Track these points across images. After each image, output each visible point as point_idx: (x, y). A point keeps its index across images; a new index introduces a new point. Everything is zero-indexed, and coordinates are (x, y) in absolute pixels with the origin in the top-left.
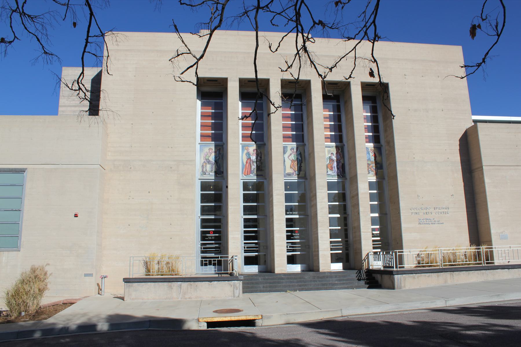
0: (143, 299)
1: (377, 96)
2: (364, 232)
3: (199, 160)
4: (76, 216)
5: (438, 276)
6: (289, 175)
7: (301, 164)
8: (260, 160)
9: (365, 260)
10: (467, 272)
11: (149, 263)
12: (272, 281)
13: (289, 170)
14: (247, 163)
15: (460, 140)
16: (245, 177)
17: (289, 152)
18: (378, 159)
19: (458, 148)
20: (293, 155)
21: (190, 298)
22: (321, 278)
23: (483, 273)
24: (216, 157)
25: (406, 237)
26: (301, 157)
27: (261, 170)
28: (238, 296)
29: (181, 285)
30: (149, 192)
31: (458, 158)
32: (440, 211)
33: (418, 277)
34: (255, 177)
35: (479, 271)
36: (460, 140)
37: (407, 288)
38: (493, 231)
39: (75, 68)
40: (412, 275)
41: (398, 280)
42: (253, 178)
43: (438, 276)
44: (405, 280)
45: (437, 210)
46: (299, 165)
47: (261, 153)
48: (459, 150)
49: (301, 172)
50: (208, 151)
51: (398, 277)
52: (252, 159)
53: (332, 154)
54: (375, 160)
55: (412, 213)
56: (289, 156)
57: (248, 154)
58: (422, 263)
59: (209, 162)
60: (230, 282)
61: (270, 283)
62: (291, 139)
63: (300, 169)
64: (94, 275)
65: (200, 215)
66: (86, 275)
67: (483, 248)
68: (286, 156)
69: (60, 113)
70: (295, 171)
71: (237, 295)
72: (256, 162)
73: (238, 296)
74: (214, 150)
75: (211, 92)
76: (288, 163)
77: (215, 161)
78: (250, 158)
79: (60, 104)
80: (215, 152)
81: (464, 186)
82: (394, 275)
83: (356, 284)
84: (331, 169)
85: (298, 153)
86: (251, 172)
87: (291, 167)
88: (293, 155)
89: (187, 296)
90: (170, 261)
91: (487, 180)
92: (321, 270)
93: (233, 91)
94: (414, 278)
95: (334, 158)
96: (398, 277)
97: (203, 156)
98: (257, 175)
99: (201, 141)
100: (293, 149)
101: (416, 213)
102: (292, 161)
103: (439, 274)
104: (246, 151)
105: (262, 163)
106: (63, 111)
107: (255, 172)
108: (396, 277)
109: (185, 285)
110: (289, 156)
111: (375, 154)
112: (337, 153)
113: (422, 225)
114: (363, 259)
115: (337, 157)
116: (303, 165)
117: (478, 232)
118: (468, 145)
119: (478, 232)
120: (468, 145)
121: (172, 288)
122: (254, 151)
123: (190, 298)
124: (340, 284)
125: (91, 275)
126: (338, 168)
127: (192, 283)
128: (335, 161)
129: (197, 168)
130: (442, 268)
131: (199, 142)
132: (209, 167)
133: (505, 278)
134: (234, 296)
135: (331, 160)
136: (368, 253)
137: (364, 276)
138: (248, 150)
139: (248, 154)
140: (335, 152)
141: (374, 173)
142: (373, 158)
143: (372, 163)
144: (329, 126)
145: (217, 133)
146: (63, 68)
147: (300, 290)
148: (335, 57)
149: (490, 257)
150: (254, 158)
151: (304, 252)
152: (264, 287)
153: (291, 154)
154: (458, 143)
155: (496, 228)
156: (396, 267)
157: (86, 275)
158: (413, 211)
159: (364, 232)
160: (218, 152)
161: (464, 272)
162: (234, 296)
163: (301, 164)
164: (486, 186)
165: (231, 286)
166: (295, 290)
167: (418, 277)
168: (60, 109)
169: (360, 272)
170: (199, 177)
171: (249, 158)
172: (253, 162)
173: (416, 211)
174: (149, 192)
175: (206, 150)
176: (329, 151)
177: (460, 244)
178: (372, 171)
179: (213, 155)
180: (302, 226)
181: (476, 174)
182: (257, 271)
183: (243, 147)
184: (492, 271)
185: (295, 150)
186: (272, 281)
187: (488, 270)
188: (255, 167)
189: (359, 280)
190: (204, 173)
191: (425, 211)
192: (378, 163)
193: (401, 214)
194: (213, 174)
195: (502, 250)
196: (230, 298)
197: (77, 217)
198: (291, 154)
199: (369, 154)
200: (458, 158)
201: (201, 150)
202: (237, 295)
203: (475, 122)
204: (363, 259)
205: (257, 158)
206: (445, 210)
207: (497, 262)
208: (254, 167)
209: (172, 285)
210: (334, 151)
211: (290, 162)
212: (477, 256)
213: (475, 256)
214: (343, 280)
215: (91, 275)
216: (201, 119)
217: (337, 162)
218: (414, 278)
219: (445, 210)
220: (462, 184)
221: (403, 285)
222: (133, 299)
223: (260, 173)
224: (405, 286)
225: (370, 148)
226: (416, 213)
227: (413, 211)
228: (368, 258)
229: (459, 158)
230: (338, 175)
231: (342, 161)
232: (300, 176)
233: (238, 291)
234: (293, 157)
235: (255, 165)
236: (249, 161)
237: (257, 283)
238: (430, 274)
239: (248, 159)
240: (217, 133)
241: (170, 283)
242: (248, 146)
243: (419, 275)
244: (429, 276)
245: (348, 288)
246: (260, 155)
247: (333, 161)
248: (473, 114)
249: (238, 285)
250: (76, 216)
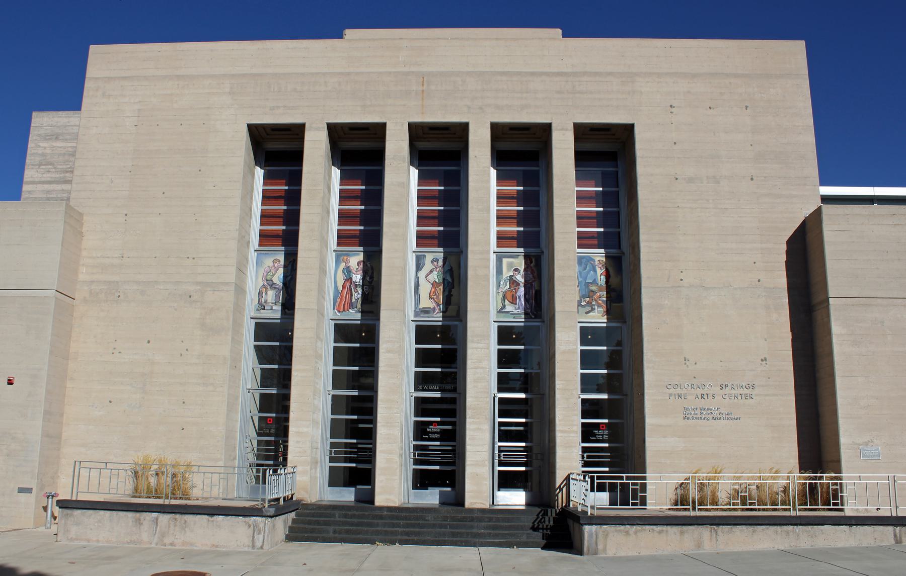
0: (88, 541)
1: (608, 151)
2: (562, 432)
3: (253, 281)
4: (10, 382)
5: (682, 533)
6: (426, 311)
7: (450, 291)
8: (370, 282)
9: (561, 490)
10: (751, 528)
11: (179, 478)
12: (356, 520)
13: (426, 303)
14: (343, 287)
15: (788, 242)
16: (339, 315)
17: (428, 266)
18: (614, 280)
19: (784, 258)
20: (435, 273)
21: (171, 544)
22: (459, 520)
23: (788, 533)
24: (285, 277)
25: (654, 444)
26: (452, 276)
27: (372, 302)
28: (262, 547)
29: (157, 519)
30: (149, 342)
31: (783, 281)
32: (733, 392)
33: (636, 533)
34: (359, 316)
35: (778, 528)
36: (790, 242)
37: (611, 553)
38: (843, 440)
39: (54, 113)
40: (622, 527)
41: (591, 535)
42: (354, 316)
43: (682, 533)
44: (606, 536)
45: (728, 391)
46: (446, 293)
47: (372, 268)
48: (787, 263)
49: (450, 307)
50: (271, 264)
51: (591, 531)
52: (354, 280)
53: (516, 270)
54: (607, 282)
55: (670, 395)
56: (428, 275)
57: (348, 270)
58: (751, 504)
59: (272, 285)
60: (247, 519)
61: (352, 524)
62: (515, 242)
63: (448, 301)
64: (34, 491)
65: (330, 389)
66: (21, 490)
67: (826, 478)
68: (422, 274)
69: (24, 195)
70: (438, 305)
71: (258, 544)
72: (363, 285)
73: (262, 547)
74: (282, 263)
75: (277, 149)
76: (425, 288)
77: (284, 284)
78: (351, 279)
79: (25, 180)
80: (285, 267)
81: (793, 341)
82: (583, 525)
83: (524, 539)
84: (513, 301)
85: (447, 268)
86: (351, 306)
87: (430, 297)
88: (435, 273)
89: (167, 541)
90: (175, 470)
91: (836, 329)
92: (468, 504)
93: (397, 146)
94: (627, 533)
95: (520, 278)
96: (591, 531)
97: (261, 273)
98: (362, 312)
99: (260, 245)
100: (437, 261)
101: (680, 396)
102: (434, 284)
103: (685, 528)
104: (343, 265)
105: (373, 288)
106: (29, 192)
107: (359, 306)
108: (587, 529)
109: (164, 518)
110: (428, 275)
111: (607, 270)
112: (525, 270)
113: (690, 422)
114: (557, 486)
115: (526, 277)
116: (454, 292)
117: (817, 443)
118: (804, 253)
119: (817, 443)
120: (804, 253)
121: (141, 524)
122: (358, 264)
123: (171, 544)
124: (490, 535)
125: (29, 490)
126: (526, 300)
127: (178, 516)
128: (522, 285)
129: (248, 298)
130: (796, 517)
131: (257, 247)
132: (271, 295)
133: (840, 545)
134: (253, 547)
135: (513, 282)
136: (569, 475)
137: (549, 522)
138: (346, 262)
139: (348, 270)
140: (522, 268)
141: (602, 310)
142: (602, 280)
143: (600, 290)
144: (515, 215)
145: (283, 228)
146: (34, 114)
147: (402, 542)
148: (490, 73)
149: (834, 497)
150: (357, 278)
151: (440, 466)
152: (335, 532)
153: (431, 271)
154: (784, 247)
155: (849, 436)
156: (694, 509)
157: (21, 490)
158: (672, 391)
159: (562, 432)
160: (290, 267)
161: (744, 527)
162: (253, 547)
163: (450, 291)
164: (835, 340)
165: (250, 526)
166: (393, 543)
167: (636, 533)
168: (25, 188)
169: (546, 514)
170: (253, 314)
171: (349, 279)
172: (356, 286)
173: (679, 391)
174: (149, 342)
175: (268, 262)
176: (510, 265)
177: (778, 463)
178: (600, 306)
179: (281, 271)
180: (440, 413)
181: (818, 315)
182: (352, 498)
183: (338, 257)
184: (810, 527)
185: (441, 263)
186: (356, 520)
187: (801, 524)
188: (360, 296)
189: (534, 529)
190: (262, 306)
191: (699, 392)
192: (614, 290)
193: (646, 397)
194: (280, 308)
195: (862, 482)
196: (246, 549)
197: (12, 384)
198: (431, 271)
199: (595, 271)
200: (781, 280)
201: (259, 263)
202: (258, 544)
203: (826, 199)
204: (557, 486)
205: (364, 279)
206: (746, 391)
207: (850, 509)
208: (357, 295)
209: (142, 518)
210: (520, 263)
211: (429, 286)
212: (810, 494)
213: (802, 494)
214: (502, 528)
215: (29, 490)
216: (263, 204)
217: (525, 287)
218: (627, 533)
219: (746, 391)
220: (789, 335)
221: (600, 547)
222: (72, 540)
223: (368, 307)
224: (605, 550)
225: (597, 259)
226: (680, 396)
227: (672, 391)
228: (568, 485)
229: (784, 280)
230: (526, 314)
231: (535, 284)
232: (448, 314)
233: (261, 537)
234: (435, 277)
235: (360, 291)
236: (348, 284)
237: (327, 524)
238: (665, 528)
239: (346, 280)
240: (283, 228)
241: (138, 515)
242: (348, 254)
243: (639, 528)
244: (660, 532)
245: (510, 545)
246: (370, 272)
247: (518, 284)
248: (823, 183)
249: (261, 526)
250: (10, 382)
